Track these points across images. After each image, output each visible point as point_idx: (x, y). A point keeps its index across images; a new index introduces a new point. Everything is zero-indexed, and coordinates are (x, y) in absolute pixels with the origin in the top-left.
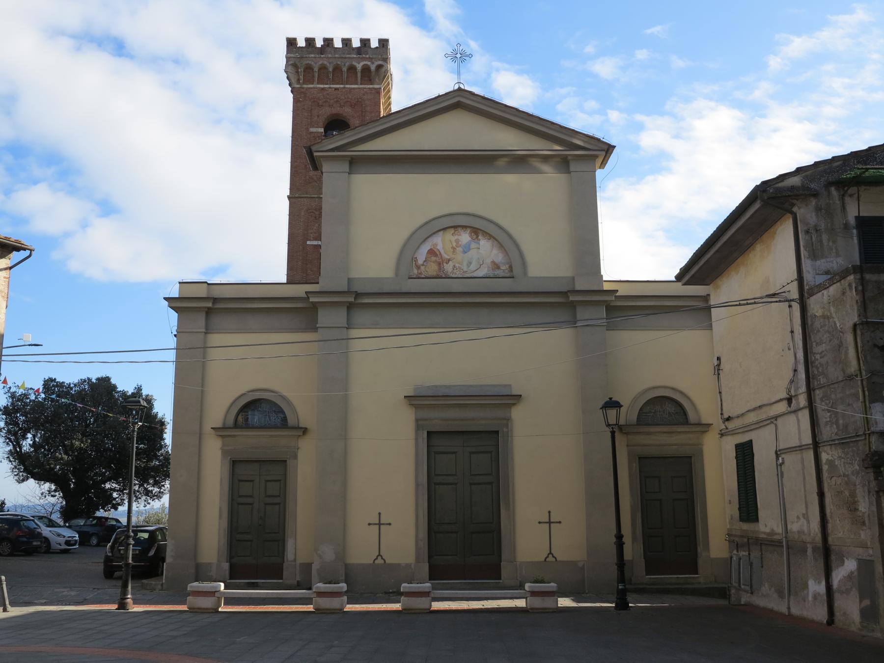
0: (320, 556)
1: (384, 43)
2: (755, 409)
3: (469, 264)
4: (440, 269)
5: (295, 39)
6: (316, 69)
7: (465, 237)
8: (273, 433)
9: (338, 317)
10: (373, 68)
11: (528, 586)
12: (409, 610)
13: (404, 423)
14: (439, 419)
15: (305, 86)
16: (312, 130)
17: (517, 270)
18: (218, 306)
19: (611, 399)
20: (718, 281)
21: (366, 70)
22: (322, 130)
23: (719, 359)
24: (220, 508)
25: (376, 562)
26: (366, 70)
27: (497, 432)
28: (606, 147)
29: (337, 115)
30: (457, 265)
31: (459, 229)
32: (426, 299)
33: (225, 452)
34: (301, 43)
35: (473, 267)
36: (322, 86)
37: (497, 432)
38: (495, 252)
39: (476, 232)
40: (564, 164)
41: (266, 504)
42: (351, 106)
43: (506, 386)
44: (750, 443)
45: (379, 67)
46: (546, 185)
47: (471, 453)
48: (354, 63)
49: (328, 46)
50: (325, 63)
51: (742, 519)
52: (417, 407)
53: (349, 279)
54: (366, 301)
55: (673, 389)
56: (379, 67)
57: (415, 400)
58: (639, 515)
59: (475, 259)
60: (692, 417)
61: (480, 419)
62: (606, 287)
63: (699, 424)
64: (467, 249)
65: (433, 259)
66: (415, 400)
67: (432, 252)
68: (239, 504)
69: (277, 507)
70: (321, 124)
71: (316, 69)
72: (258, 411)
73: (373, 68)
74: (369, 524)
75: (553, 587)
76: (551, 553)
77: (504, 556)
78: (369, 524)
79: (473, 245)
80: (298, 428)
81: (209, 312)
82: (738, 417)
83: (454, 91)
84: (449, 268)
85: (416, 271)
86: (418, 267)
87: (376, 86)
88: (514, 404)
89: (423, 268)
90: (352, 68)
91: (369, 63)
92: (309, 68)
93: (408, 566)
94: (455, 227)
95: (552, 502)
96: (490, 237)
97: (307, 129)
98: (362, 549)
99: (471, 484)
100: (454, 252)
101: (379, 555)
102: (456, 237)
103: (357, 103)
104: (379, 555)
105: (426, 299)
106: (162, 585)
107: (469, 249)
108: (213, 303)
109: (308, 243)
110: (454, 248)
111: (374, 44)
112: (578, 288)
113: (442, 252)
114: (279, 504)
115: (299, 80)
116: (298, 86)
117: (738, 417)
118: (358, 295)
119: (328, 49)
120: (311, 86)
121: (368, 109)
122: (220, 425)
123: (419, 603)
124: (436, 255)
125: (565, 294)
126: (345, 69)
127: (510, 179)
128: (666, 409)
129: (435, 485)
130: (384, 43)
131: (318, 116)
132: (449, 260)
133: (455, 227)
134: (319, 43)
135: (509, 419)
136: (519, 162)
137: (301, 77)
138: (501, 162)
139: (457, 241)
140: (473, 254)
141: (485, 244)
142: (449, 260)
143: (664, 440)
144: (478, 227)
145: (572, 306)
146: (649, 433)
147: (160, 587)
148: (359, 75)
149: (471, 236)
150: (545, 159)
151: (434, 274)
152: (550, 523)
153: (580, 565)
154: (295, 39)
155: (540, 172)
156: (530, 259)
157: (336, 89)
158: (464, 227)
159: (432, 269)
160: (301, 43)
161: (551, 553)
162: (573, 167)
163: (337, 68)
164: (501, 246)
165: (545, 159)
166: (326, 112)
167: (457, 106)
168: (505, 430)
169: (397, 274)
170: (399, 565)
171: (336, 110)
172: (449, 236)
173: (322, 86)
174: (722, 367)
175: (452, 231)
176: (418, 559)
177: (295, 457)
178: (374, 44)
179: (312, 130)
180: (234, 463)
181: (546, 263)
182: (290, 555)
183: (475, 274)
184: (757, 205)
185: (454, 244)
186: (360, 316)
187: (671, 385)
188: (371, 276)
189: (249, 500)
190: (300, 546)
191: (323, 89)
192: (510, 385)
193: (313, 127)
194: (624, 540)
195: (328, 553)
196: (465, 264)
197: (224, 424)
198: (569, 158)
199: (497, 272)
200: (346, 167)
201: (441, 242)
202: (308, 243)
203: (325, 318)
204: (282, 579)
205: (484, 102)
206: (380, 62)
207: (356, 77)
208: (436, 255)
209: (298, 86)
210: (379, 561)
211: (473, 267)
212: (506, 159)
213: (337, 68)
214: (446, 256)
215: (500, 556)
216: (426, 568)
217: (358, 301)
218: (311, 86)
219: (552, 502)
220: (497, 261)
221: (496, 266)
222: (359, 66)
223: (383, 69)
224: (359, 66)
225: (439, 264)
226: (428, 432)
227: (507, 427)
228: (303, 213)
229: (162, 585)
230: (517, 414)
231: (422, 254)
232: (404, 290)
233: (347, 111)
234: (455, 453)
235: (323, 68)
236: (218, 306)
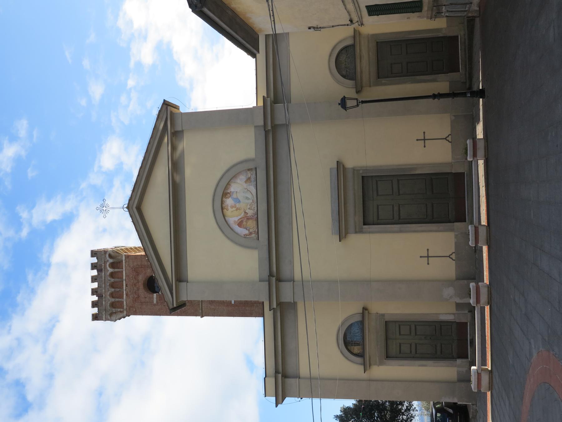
0: (451, 297)
1: (94, 254)
2: (345, 5)
3: (247, 198)
4: (251, 219)
5: (93, 315)
6: (113, 300)
7: (229, 202)
8: (367, 331)
9: (286, 287)
10: (111, 261)
11: (469, 159)
12: (487, 240)
13: (360, 241)
14: (355, 217)
15: (125, 307)
16: (155, 302)
17: (251, 165)
18: (280, 370)
19: (339, 104)
20: (256, 30)
21: (112, 265)
22: (155, 295)
23: (310, 28)
24: (419, 366)
25: (454, 259)
26: (112, 265)
27: (363, 177)
28: (165, 106)
29: (144, 284)
30: (248, 207)
31: (223, 206)
32: (272, 228)
33: (381, 363)
34: (95, 310)
35: (249, 196)
36: (125, 296)
37: (363, 177)
38: (238, 181)
39: (225, 194)
40: (177, 135)
41: (416, 335)
43: (331, 172)
44: (367, 7)
45: (110, 256)
46: (191, 146)
47: (378, 195)
48: (108, 273)
49: (97, 292)
50: (108, 293)
51: (420, 11)
52: (347, 233)
53: (260, 281)
54: (275, 269)
55: (330, 56)
56: (110, 256)
57: (342, 234)
58: (418, 78)
59: (244, 196)
60: (350, 42)
61: (354, 189)
62: (261, 104)
63: (354, 37)
64: (237, 201)
65: (244, 223)
66: (342, 234)
67: (240, 224)
68: (416, 353)
69: (417, 327)
70: (151, 296)
71: (113, 300)
72: (352, 341)
73: (111, 261)
74: (428, 264)
75: (470, 143)
76: (446, 139)
77: (448, 170)
78: (428, 264)
79: (234, 196)
80: (363, 314)
81: (285, 376)
82: (350, 15)
83: (129, 211)
84: (250, 213)
85: (253, 235)
86: (251, 233)
87: (124, 258)
88: (343, 166)
89: (251, 230)
90: (112, 275)
91: (108, 263)
92: (113, 305)
93: (456, 236)
94: (222, 209)
95: (411, 138)
96: (228, 184)
97: (155, 305)
98: (446, 269)
99: (399, 194)
100: (239, 209)
101: (449, 257)
102: (229, 208)
103: (136, 271)
104: (449, 257)
105: (272, 228)
106: (473, 405)
107: (237, 198)
108: (279, 373)
110: (237, 209)
111: (95, 260)
112: (262, 123)
113: (239, 217)
114: (415, 326)
115: (121, 312)
116: (125, 312)
117: (350, 15)
118: (271, 275)
119: (99, 291)
121: (139, 263)
122: (362, 367)
123: (483, 233)
124: (242, 222)
125: (267, 132)
126: (112, 280)
127: (188, 171)
128: (345, 61)
129: (400, 219)
130: (94, 254)
131: (145, 298)
132: (245, 212)
133: (222, 209)
134: (95, 298)
135: (354, 169)
136: (176, 166)
137: (119, 310)
138: (177, 178)
139: (232, 207)
140: (240, 196)
141: (233, 188)
142: (245, 212)
143: (366, 62)
144: (222, 193)
145: (275, 127)
146: (361, 72)
147: (474, 406)
148: (116, 270)
149: (228, 198)
150: (174, 148)
151: (255, 222)
152: (424, 140)
153: (453, 118)
154: (93, 315)
155: (183, 152)
156: (242, 156)
157: (126, 286)
158: (222, 202)
159: (251, 224)
160: (95, 310)
161: (446, 139)
162: (179, 128)
163: (112, 285)
164: (235, 177)
165: (174, 148)
166: (143, 292)
167: (139, 209)
168: (361, 172)
169: (256, 248)
170: (456, 243)
171: (141, 285)
172: (229, 212)
173: (125, 296)
174: (315, 26)
175: (225, 211)
176: (452, 230)
177: (383, 315)
178: (95, 260)
179: (155, 302)
180: (388, 356)
181: (245, 146)
182: (451, 318)
183: (255, 194)
184: (205, 10)
185: (234, 209)
186: (285, 272)
187: (327, 58)
188: (257, 266)
189: (413, 347)
190: (444, 311)
191: (127, 295)
192: (330, 169)
194: (436, 93)
195: (449, 292)
196: (247, 201)
197: (361, 364)
198: (173, 131)
199: (253, 179)
200: (183, 285)
201: (233, 219)
203: (287, 297)
204: (467, 323)
205: (136, 191)
206: (107, 255)
207: (118, 272)
208: (242, 222)
209: (125, 312)
210: (453, 256)
211: (249, 196)
212: (175, 175)
213: (112, 285)
214: (243, 215)
215: (448, 173)
216: (457, 225)
217: (275, 274)
218: (125, 303)
219: (411, 138)
220: (245, 180)
221: (248, 180)
222: (110, 270)
223: (112, 253)
224: (110, 270)
225: (248, 219)
226: (364, 224)
227: (358, 170)
229: (473, 405)
230: (350, 164)
231: (242, 231)
232: (266, 243)
233: (142, 278)
234: (378, 206)
235: (112, 295)
236: (280, 370)
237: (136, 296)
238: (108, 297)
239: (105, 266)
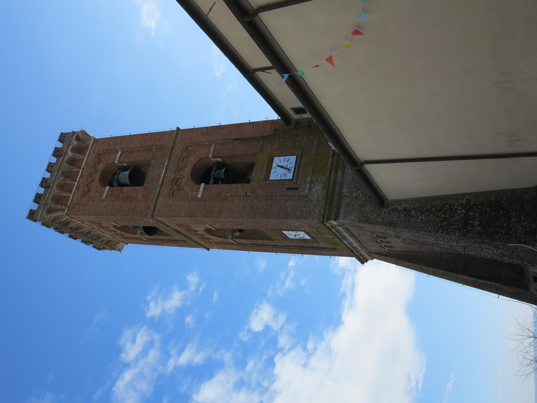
21: (76, 150)
26: (76, 150)
34: (35, 207)
36: (75, 188)
42: (99, 163)
45: (78, 139)
48: (66, 158)
49: (46, 182)
91: (71, 146)
97: (102, 201)
103: (99, 157)
109: (199, 196)
120: (71, 198)
131: (96, 192)
134: (42, 191)
166: (95, 185)
179: (104, 197)
191: (77, 188)
193: (102, 196)
202: (199, 196)
224: (70, 154)
228: (171, 202)
237: (87, 190)
238: (55, 187)
239: (67, 150)
